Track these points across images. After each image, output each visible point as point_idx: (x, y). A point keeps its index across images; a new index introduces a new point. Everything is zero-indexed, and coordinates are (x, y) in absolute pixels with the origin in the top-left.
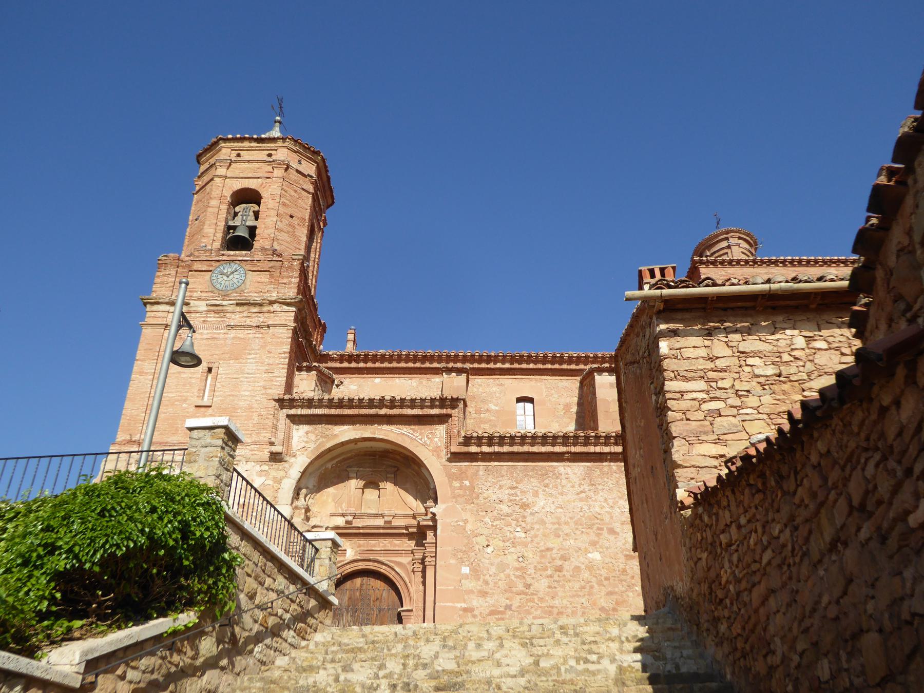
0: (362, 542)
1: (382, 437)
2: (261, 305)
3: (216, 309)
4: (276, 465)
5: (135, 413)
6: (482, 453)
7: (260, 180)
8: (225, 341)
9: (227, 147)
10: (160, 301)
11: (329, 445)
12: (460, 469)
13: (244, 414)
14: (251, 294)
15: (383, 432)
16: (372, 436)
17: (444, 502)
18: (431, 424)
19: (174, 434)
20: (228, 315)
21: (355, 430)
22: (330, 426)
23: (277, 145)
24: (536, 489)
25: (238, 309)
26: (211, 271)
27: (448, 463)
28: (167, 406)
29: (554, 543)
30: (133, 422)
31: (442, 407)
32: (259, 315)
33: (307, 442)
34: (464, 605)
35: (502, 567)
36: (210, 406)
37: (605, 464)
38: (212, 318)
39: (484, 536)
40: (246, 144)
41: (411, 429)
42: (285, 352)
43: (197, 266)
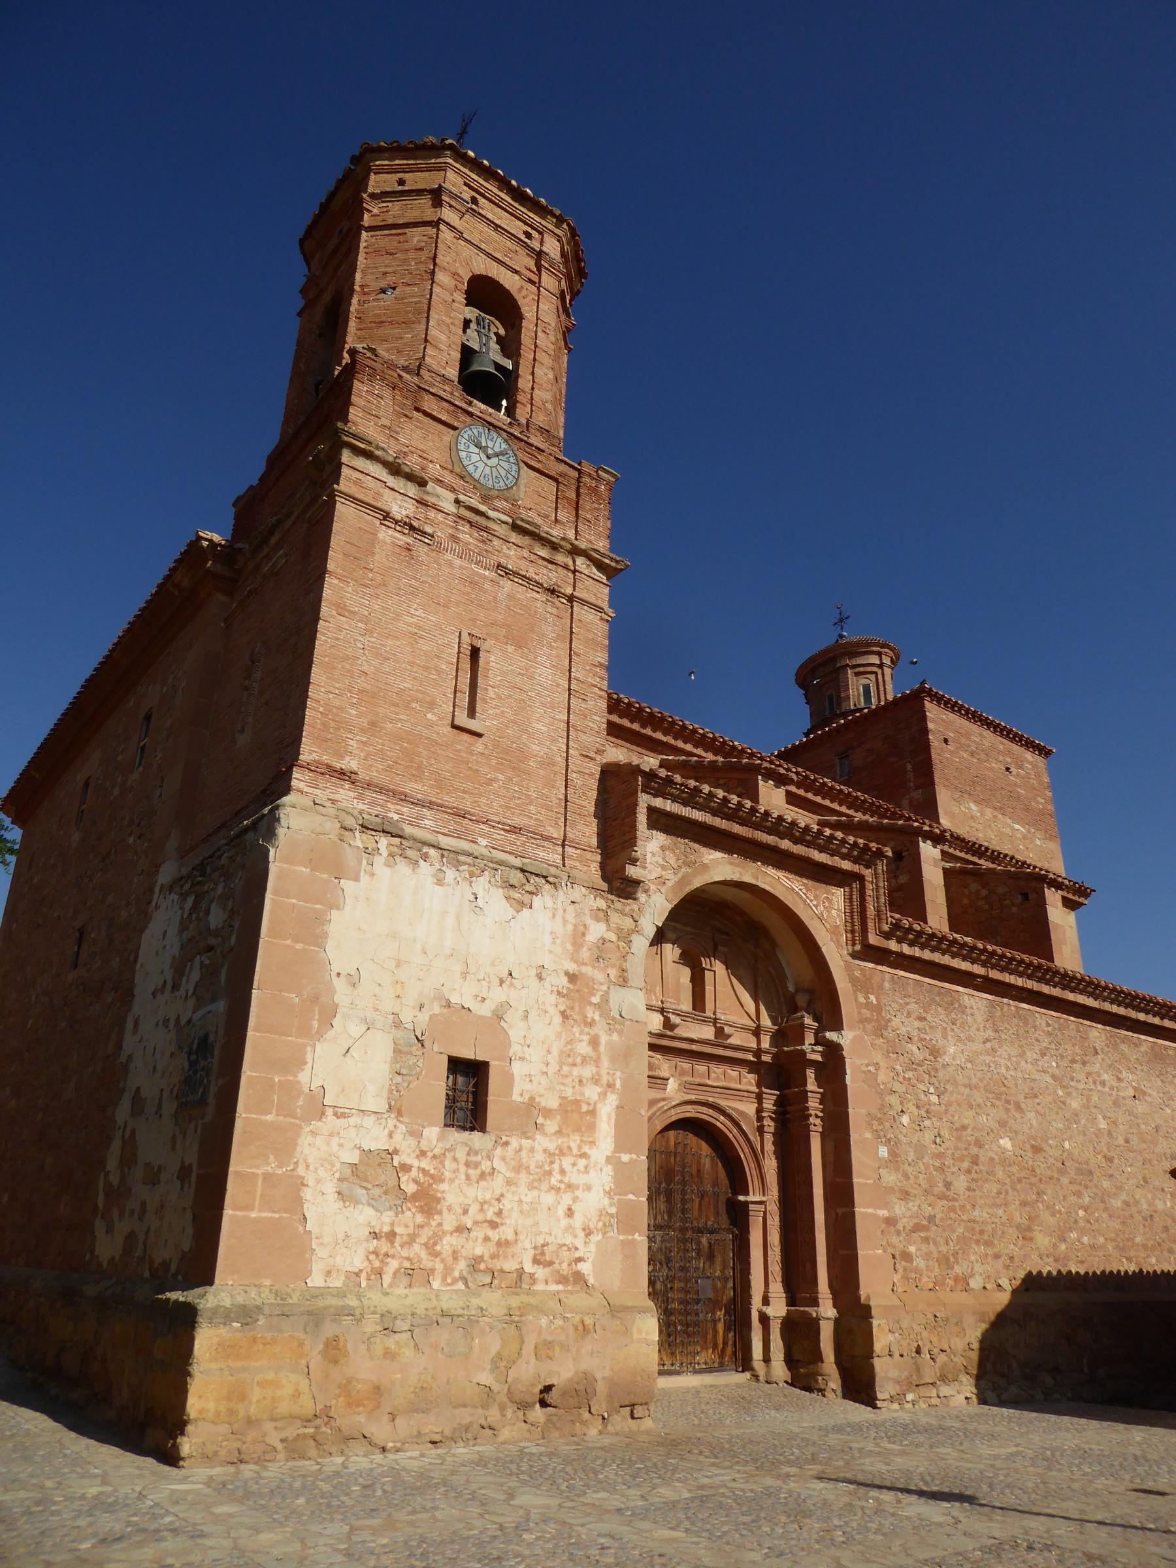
0: (686, 1065)
1: (767, 888)
2: (554, 547)
3: (474, 518)
4: (619, 904)
5: (337, 703)
6: (901, 955)
7: (517, 277)
8: (495, 598)
9: (458, 172)
10: (378, 453)
11: (697, 883)
12: (863, 970)
13: (541, 772)
14: (531, 513)
15: (768, 879)
16: (753, 882)
17: (851, 1028)
18: (827, 884)
19: (416, 778)
20: (496, 542)
21: (731, 864)
22: (696, 846)
23: (544, 222)
24: (945, 1025)
25: (514, 537)
26: (454, 428)
27: (849, 959)
28: (397, 705)
29: (967, 1117)
30: (332, 724)
31: (855, 861)
32: (550, 566)
33: (663, 867)
34: (884, 1213)
35: (920, 1149)
36: (480, 735)
37: (1005, 1000)
38: (466, 535)
39: (897, 1094)
40: (492, 187)
41: (804, 884)
42: (601, 665)
43: (429, 404)
